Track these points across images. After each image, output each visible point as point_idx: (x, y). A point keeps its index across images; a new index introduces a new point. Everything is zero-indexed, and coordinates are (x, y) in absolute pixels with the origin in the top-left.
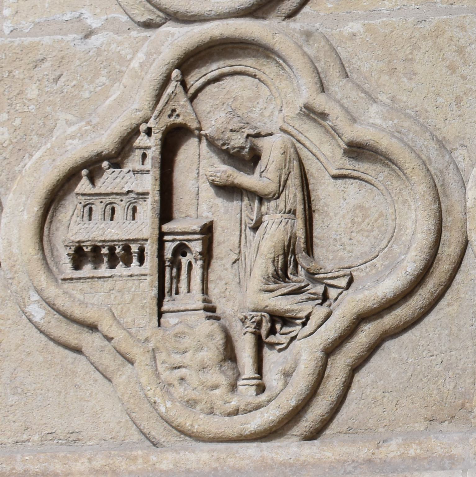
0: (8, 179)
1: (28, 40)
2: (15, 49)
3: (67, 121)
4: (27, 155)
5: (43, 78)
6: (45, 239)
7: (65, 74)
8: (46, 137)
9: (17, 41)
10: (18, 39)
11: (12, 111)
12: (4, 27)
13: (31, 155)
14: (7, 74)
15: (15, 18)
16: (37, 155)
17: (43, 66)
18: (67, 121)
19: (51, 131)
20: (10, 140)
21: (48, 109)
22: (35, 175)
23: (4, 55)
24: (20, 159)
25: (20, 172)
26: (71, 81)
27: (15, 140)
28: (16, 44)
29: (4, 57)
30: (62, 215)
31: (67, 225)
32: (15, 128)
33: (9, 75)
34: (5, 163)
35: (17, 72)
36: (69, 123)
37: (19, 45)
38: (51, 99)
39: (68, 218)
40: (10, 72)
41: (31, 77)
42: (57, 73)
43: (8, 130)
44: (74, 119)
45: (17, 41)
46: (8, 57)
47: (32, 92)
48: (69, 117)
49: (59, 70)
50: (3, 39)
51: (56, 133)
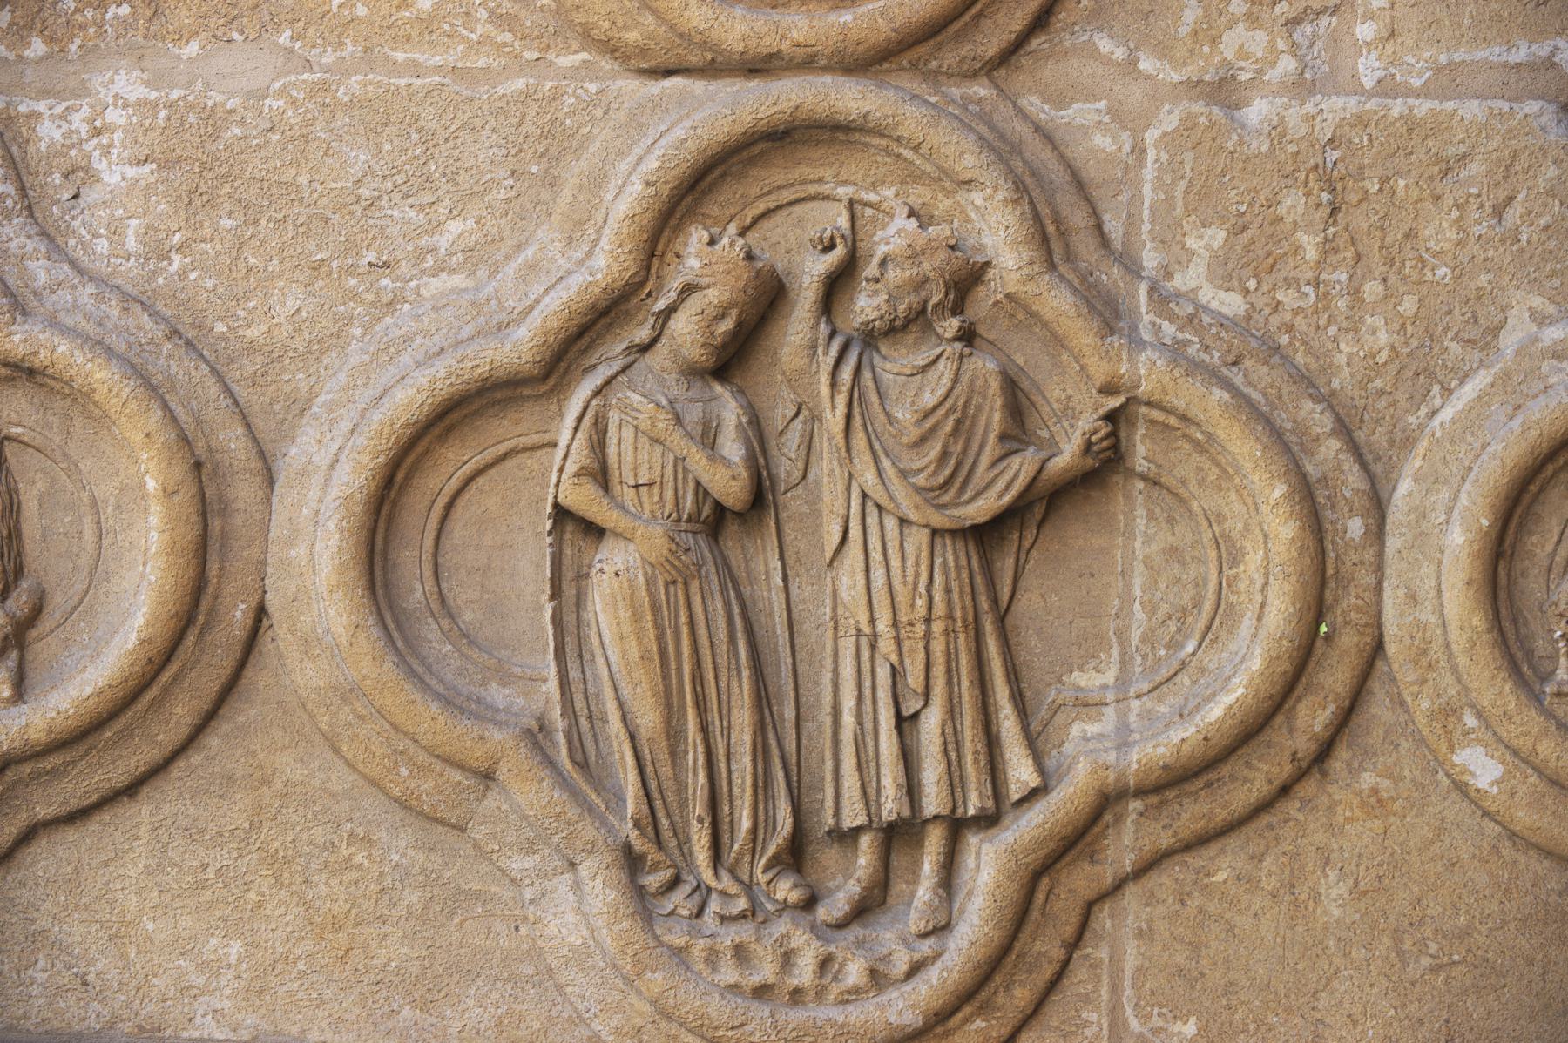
0: (1391, 443)
1: (1423, 107)
2: (1393, 124)
3: (1533, 313)
4: (1436, 388)
5: (1467, 202)
6: (1502, 595)
7: (1520, 197)
8: (1482, 350)
9: (1397, 108)
10: (1399, 101)
11: (1393, 279)
12: (1361, 68)
13: (1448, 392)
14: (1377, 187)
15: (1390, 48)
16: (1469, 391)
17: (1464, 174)
18: (1533, 313)
19: (1495, 331)
20: (1393, 348)
21: (1483, 280)
22: (1469, 438)
23: (1365, 138)
24: (1418, 398)
25: (1422, 427)
26: (1540, 215)
27: (1405, 350)
28: (1395, 112)
29: (1365, 142)
30: (1534, 539)
31: (1546, 563)
32: (1401, 321)
33: (1380, 190)
34: (1384, 404)
35: (1402, 183)
36: (1541, 320)
37: (1401, 117)
38: (1491, 253)
39: (1549, 548)
40: (1384, 181)
41: (1438, 198)
42: (1502, 194)
43: (1386, 323)
44: (1551, 309)
45: (1397, 108)
46: (1376, 144)
47: (1439, 231)
48: (1537, 302)
49: (1506, 186)
50: (1363, 99)
51: (1509, 341)
